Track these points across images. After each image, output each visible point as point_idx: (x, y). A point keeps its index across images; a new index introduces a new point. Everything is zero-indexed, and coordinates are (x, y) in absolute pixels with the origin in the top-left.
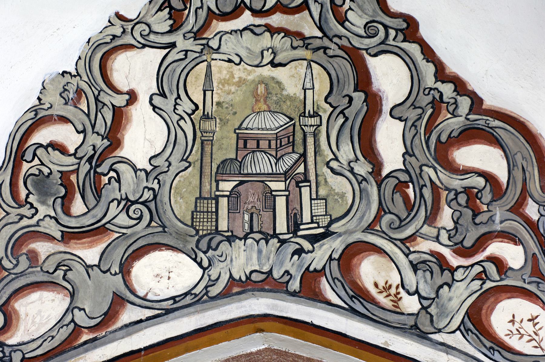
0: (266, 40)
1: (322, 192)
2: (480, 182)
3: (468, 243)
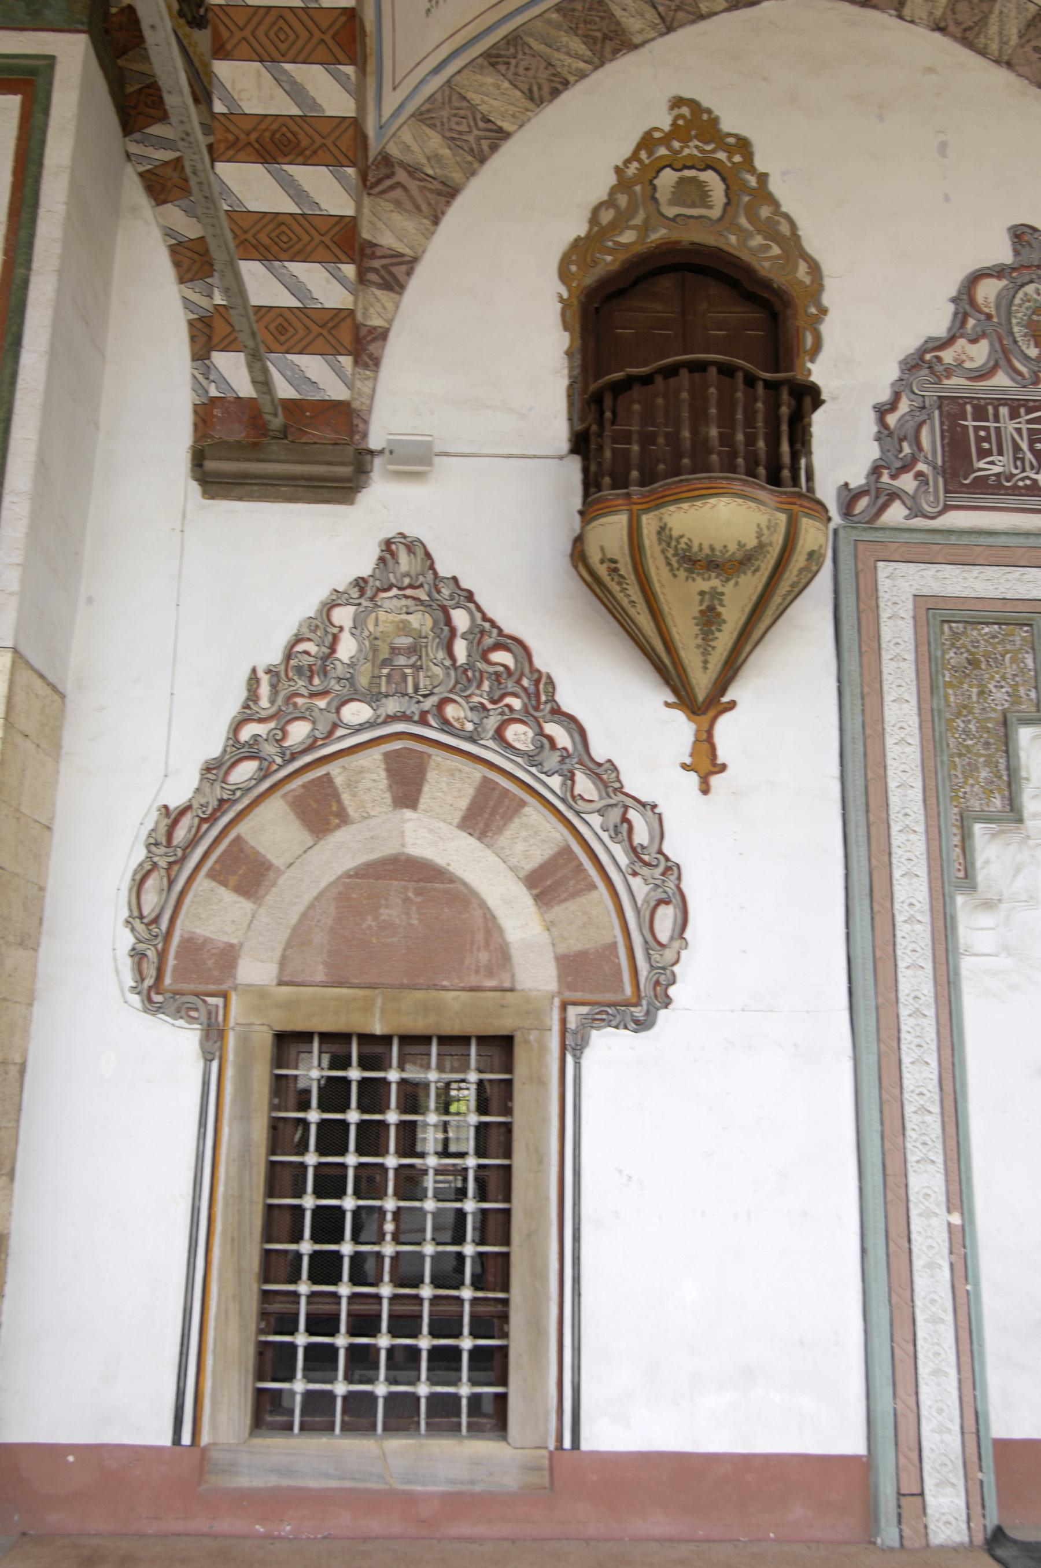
0: (404, 602)
1: (429, 674)
2: (501, 669)
3: (496, 698)
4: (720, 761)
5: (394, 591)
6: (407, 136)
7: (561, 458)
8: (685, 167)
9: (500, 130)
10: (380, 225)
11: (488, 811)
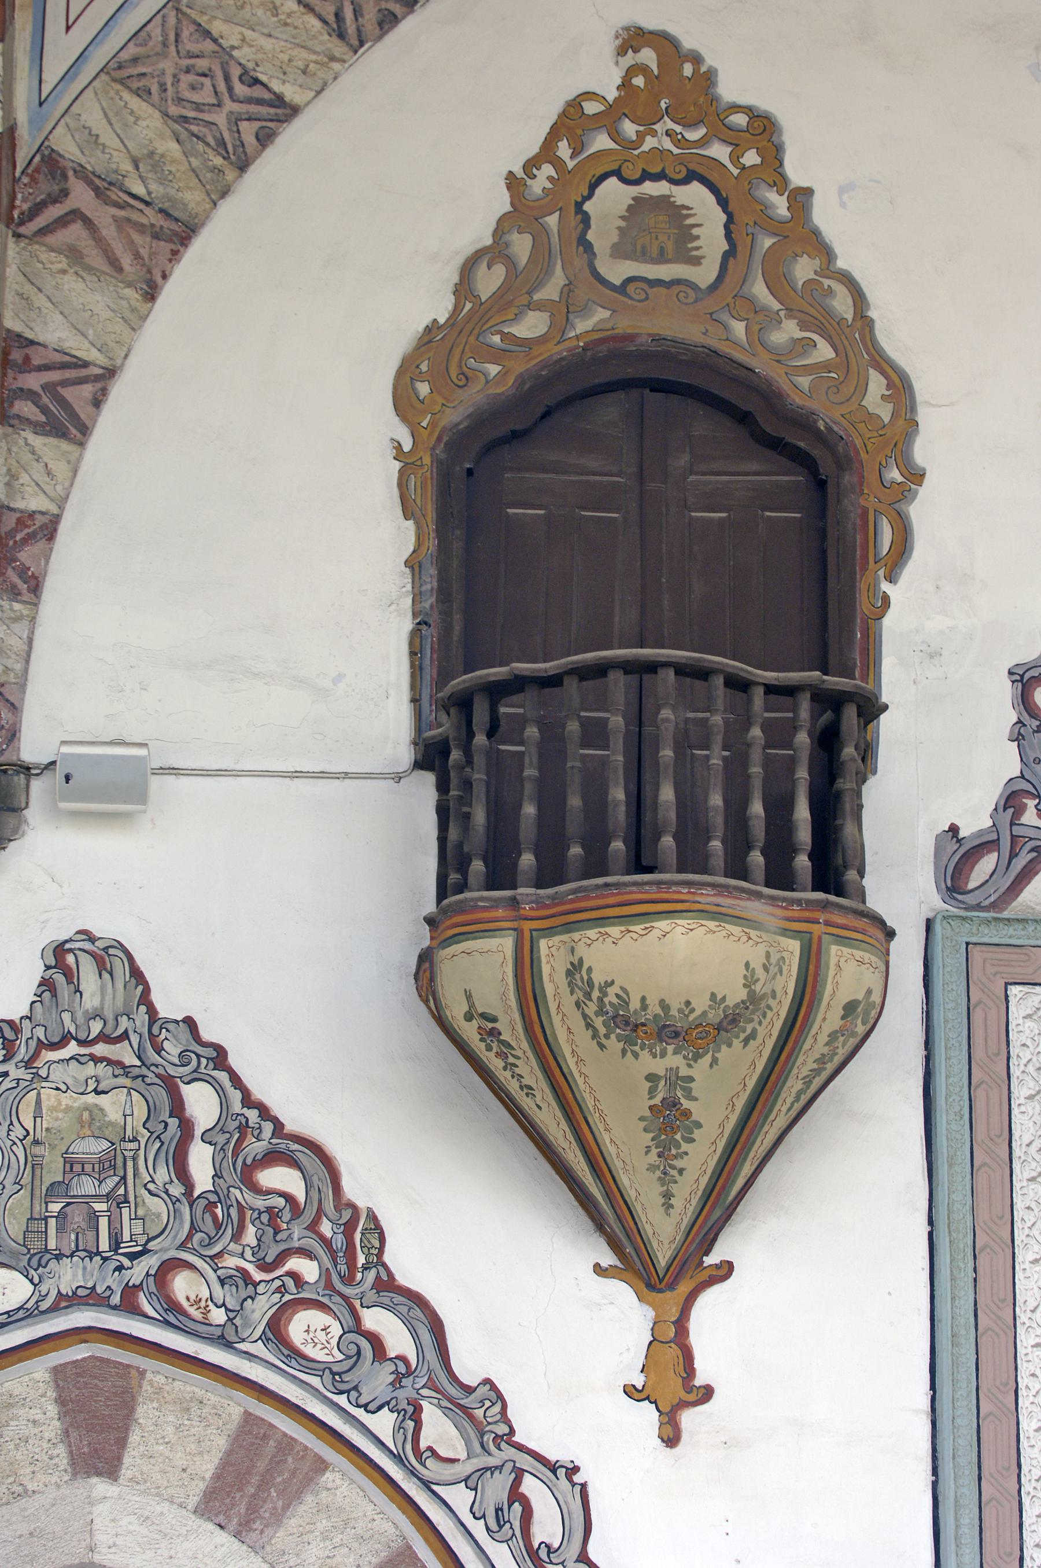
0: (90, 1069)
1: (141, 1212)
2: (281, 1202)
3: (269, 1259)
4: (698, 1382)
5: (72, 1048)
6: (91, 114)
7: (398, 778)
8: (646, 176)
9: (278, 101)
10: (40, 300)
11: (255, 1480)
